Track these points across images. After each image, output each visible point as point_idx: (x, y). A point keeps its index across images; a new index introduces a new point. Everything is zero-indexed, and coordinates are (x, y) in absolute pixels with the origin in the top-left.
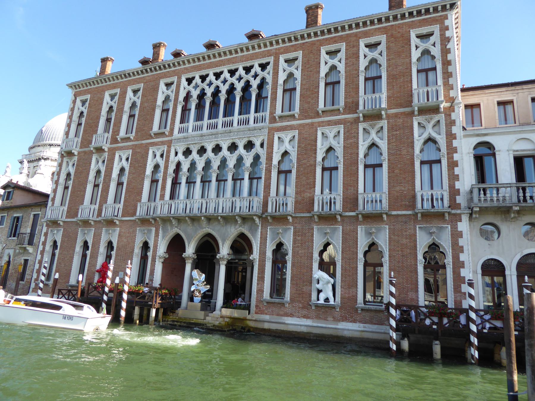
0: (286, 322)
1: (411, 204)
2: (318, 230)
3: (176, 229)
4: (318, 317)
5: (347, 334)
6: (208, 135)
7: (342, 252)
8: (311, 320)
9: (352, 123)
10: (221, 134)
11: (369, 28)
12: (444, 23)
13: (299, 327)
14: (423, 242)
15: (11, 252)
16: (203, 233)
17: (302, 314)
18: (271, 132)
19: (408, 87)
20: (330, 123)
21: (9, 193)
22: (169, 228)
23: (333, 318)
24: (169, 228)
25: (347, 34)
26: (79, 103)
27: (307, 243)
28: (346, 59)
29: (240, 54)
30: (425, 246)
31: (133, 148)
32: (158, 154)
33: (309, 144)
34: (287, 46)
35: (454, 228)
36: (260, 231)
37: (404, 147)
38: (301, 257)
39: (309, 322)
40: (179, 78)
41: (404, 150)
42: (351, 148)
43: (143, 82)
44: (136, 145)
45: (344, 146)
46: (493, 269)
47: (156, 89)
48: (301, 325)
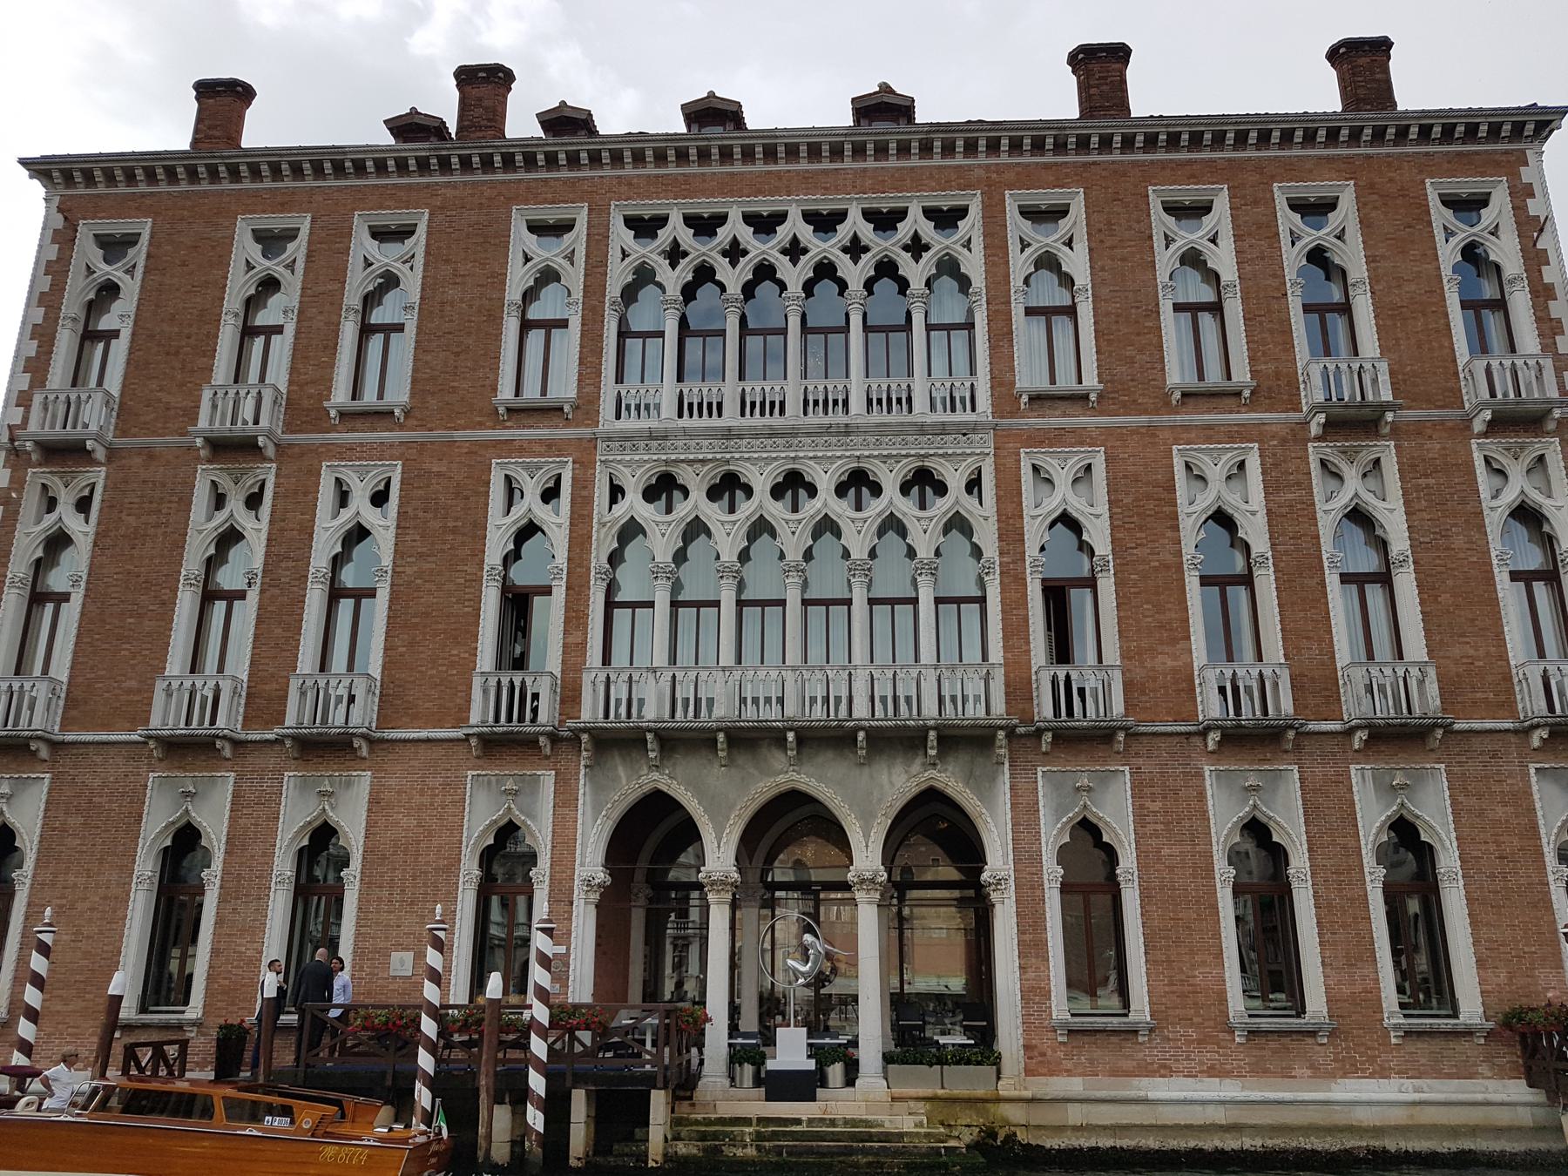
0: (1152, 1095)
1: (1503, 698)
2: (1218, 777)
3: (655, 775)
4: (1259, 1070)
5: (1364, 1117)
6: (756, 436)
7: (1310, 850)
8: (1238, 1082)
10: (809, 434)
11: (1296, 152)
12: (1514, 176)
13: (1198, 1108)
16: (774, 792)
17: (1201, 1063)
18: (1007, 444)
19: (1441, 347)
20: (1209, 433)
22: (621, 771)
23: (1312, 1067)
24: (621, 771)
25: (1229, 160)
27: (1187, 823)
28: (1238, 238)
29: (848, 163)
32: (532, 488)
33: (1149, 497)
34: (1028, 165)
37: (1455, 525)
38: (1171, 869)
39: (1230, 1090)
41: (1458, 534)
42: (1291, 517)
43: (427, 205)
44: (423, 444)
45: (1269, 512)
48: (1204, 1103)
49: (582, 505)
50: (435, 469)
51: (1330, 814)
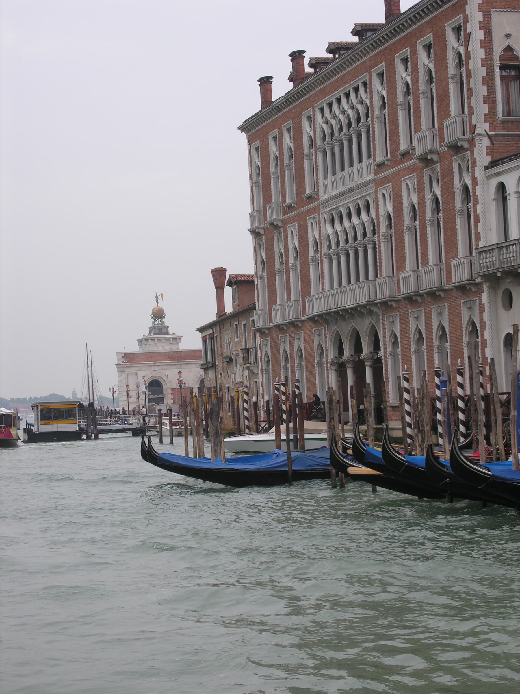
9: (421, 169)
12: (465, 11)
30: (467, 325)
35: (480, 300)
36: (381, 321)
50: (302, 223)
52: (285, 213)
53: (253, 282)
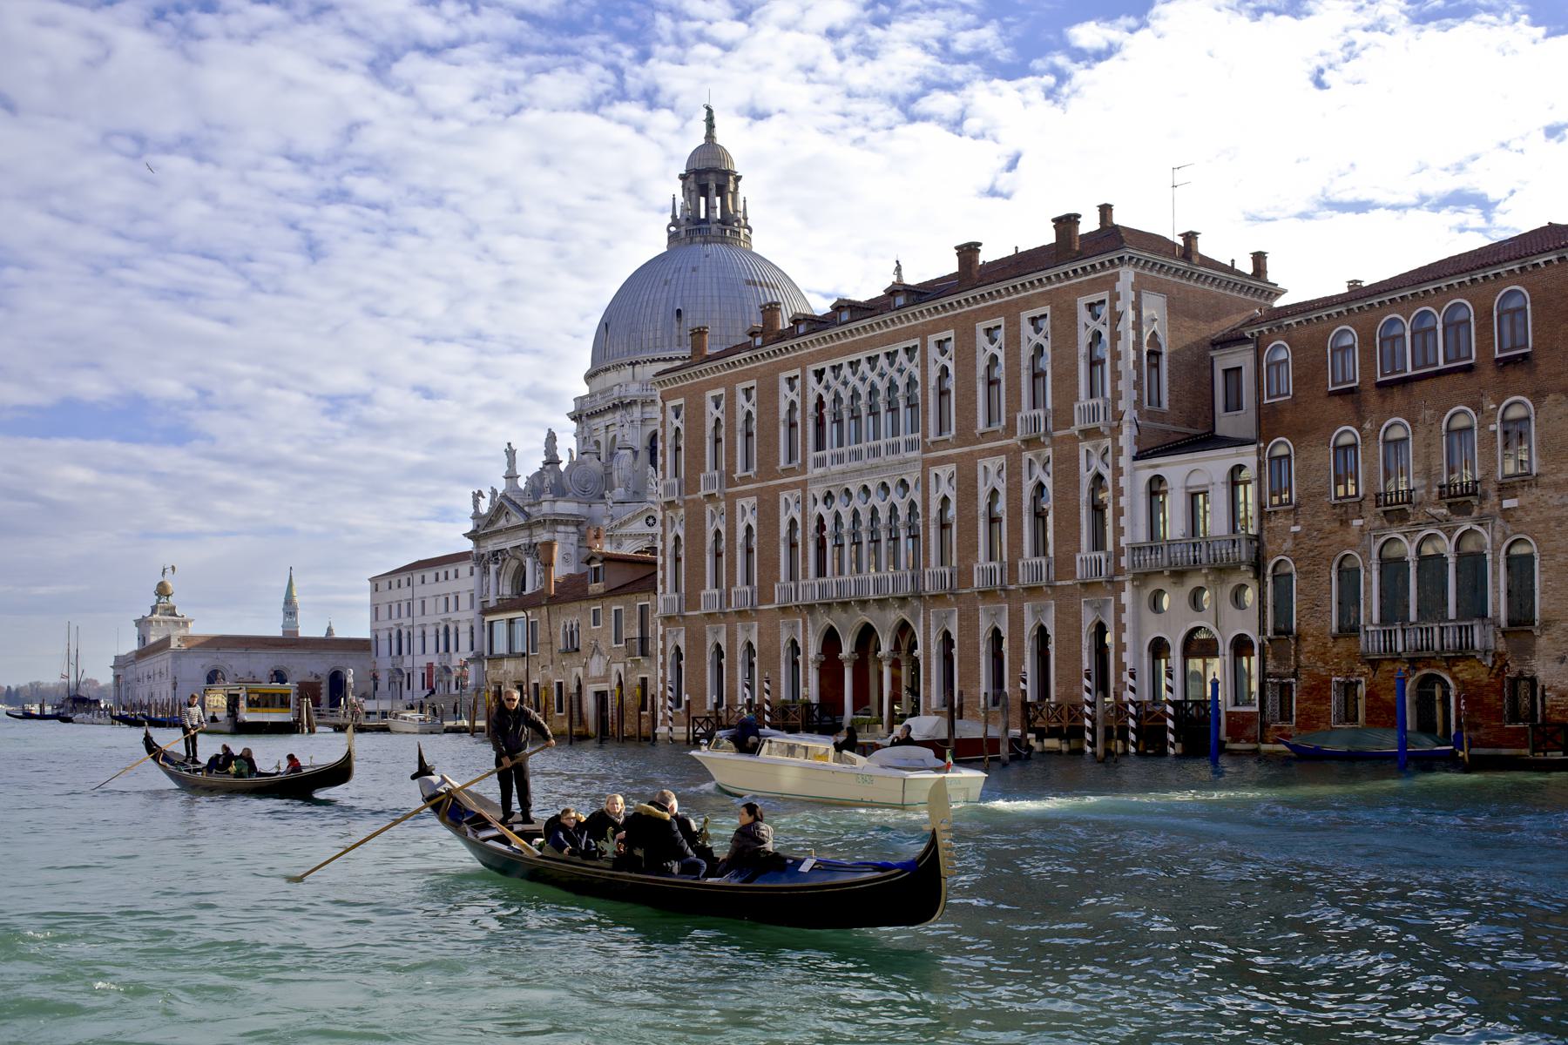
14: (1088, 619)
15: (621, 667)
18: (927, 464)
21: (596, 569)
26: (671, 414)
31: (757, 492)
35: (1118, 600)
40: (804, 371)
46: (1159, 648)
47: (774, 391)
49: (804, 508)
51: (1016, 621)
52: (731, 482)
53: (654, 563)
